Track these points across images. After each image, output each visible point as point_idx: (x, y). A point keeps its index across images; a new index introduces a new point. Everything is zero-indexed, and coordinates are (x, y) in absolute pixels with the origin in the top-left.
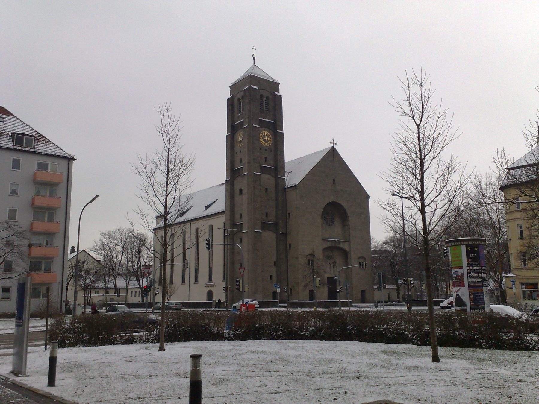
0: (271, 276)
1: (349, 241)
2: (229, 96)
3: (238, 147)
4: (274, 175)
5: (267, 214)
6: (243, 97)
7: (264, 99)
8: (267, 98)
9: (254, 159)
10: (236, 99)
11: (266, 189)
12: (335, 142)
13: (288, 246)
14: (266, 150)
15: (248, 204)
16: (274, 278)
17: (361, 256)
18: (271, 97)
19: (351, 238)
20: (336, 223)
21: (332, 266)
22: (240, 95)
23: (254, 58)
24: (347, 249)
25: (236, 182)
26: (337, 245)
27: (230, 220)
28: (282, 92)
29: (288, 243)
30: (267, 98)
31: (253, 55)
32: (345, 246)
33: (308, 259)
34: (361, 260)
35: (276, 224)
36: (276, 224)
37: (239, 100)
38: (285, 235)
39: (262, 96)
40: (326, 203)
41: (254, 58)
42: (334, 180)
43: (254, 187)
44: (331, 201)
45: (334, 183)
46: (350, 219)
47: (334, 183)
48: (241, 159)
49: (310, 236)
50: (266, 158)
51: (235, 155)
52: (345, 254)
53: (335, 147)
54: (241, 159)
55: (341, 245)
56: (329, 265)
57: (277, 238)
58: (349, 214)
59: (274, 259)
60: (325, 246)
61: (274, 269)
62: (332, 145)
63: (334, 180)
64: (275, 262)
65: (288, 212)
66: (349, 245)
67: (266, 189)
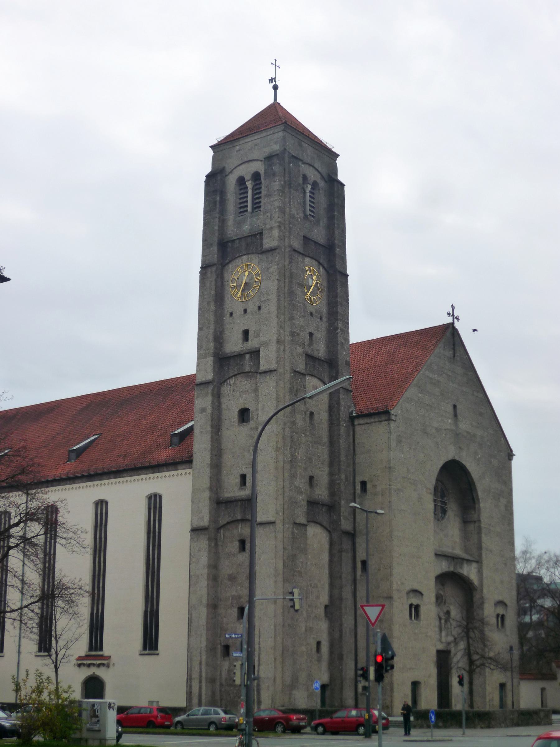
0: (319, 643)
1: (479, 562)
2: (208, 169)
3: (235, 297)
5: (311, 478)
6: (256, 177)
7: (309, 188)
8: (315, 185)
9: (293, 334)
10: (232, 181)
12: (456, 315)
13: (359, 565)
14: (311, 314)
15: (277, 449)
16: (325, 649)
17: (500, 598)
21: (443, 621)
22: (246, 171)
23: (275, 88)
24: (476, 582)
25: (226, 389)
27: (211, 489)
29: (361, 555)
30: (315, 185)
31: (272, 80)
33: (409, 602)
34: (501, 611)
35: (332, 507)
37: (241, 181)
38: (352, 536)
39: (305, 178)
40: (441, 463)
41: (275, 88)
42: (455, 406)
45: (455, 415)
46: (482, 505)
47: (455, 415)
48: (246, 333)
49: (412, 544)
50: (311, 335)
51: (227, 319)
53: (457, 325)
54: (246, 333)
57: (331, 544)
58: (480, 494)
59: (325, 599)
61: (324, 625)
62: (449, 320)
63: (455, 406)
64: (326, 607)
65: (359, 479)
66: (480, 572)
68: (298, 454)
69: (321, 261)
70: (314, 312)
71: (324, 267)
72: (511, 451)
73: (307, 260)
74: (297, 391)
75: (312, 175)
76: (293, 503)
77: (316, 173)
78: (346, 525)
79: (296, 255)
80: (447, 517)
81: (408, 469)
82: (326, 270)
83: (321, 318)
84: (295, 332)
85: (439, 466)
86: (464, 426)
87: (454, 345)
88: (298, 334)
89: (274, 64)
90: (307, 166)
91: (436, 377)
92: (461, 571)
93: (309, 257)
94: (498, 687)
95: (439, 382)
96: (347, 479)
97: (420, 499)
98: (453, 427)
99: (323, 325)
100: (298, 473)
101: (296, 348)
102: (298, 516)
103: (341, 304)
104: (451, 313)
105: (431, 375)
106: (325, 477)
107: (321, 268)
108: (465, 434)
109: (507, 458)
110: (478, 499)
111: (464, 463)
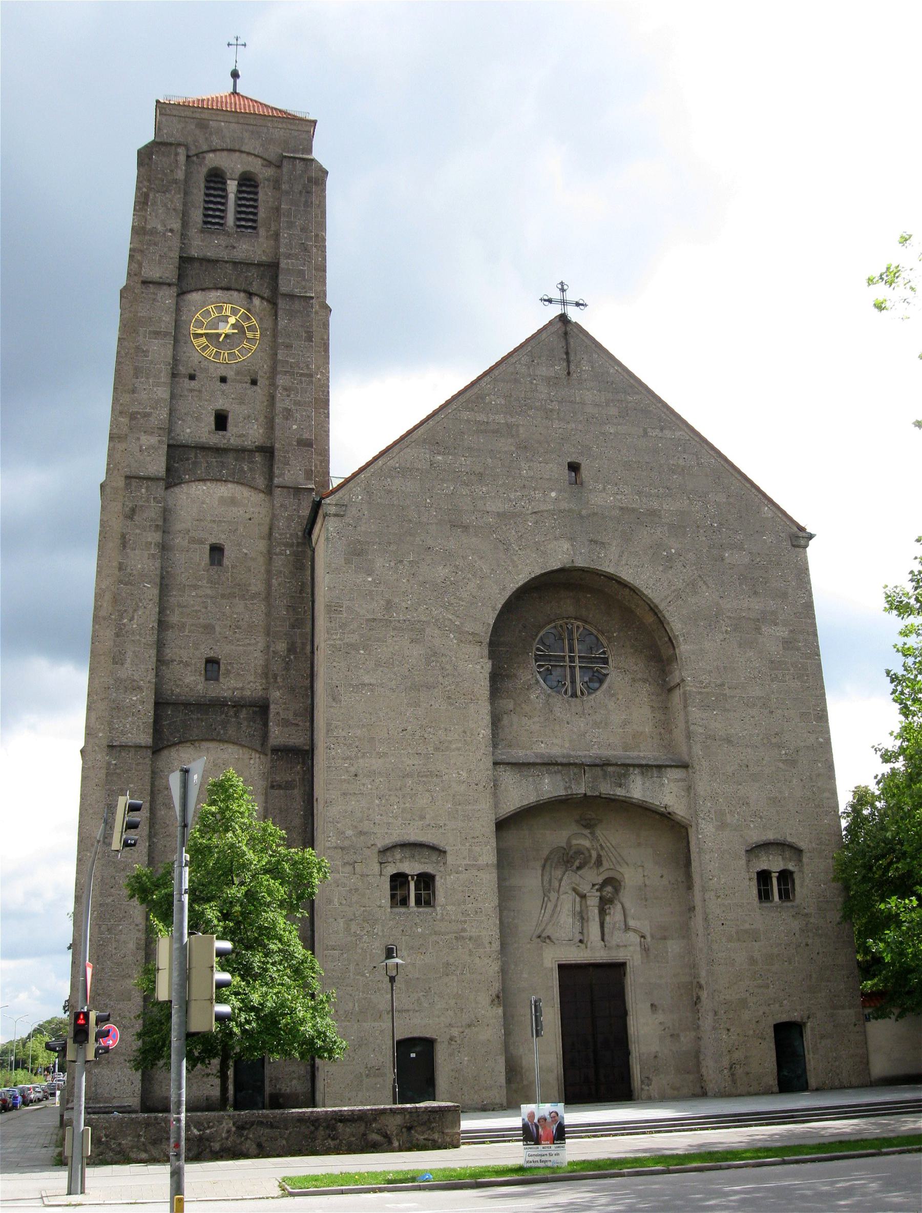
4: (261, 482)
7: (232, 186)
11: (217, 551)
14: (223, 380)
17: (771, 836)
18: (263, 173)
19: (697, 750)
20: (615, 678)
21: (593, 902)
26: (606, 788)
28: (321, 152)
32: (667, 794)
33: (391, 870)
35: (261, 709)
36: (261, 709)
40: (522, 579)
41: (235, 75)
42: (574, 467)
43: (123, 536)
44: (555, 565)
52: (672, 830)
53: (574, 315)
55: (638, 789)
56: (568, 902)
60: (519, 793)
62: (555, 311)
63: (574, 467)
67: (217, 551)
68: (131, 619)
69: (254, 288)
70: (230, 374)
71: (262, 298)
72: (802, 529)
73: (214, 294)
74: (133, 510)
75: (234, 165)
76: (117, 708)
77: (251, 158)
78: (277, 735)
79: (152, 288)
80: (605, 686)
81: (389, 602)
82: (268, 301)
83: (254, 382)
84: (137, 413)
85: (513, 586)
86: (602, 497)
87: (567, 353)
88: (147, 415)
89: (237, 43)
90: (225, 153)
91: (501, 419)
92: (620, 792)
93: (217, 289)
94: (770, 1033)
95: (509, 426)
96: (291, 649)
97: (433, 654)
98: (564, 505)
99: (260, 392)
100: (130, 654)
101: (138, 439)
102: (123, 733)
103: (289, 346)
104: (557, 295)
105: (482, 417)
106: (258, 654)
107: (256, 301)
108: (617, 512)
109: (786, 544)
110: (676, 637)
111: (611, 570)
